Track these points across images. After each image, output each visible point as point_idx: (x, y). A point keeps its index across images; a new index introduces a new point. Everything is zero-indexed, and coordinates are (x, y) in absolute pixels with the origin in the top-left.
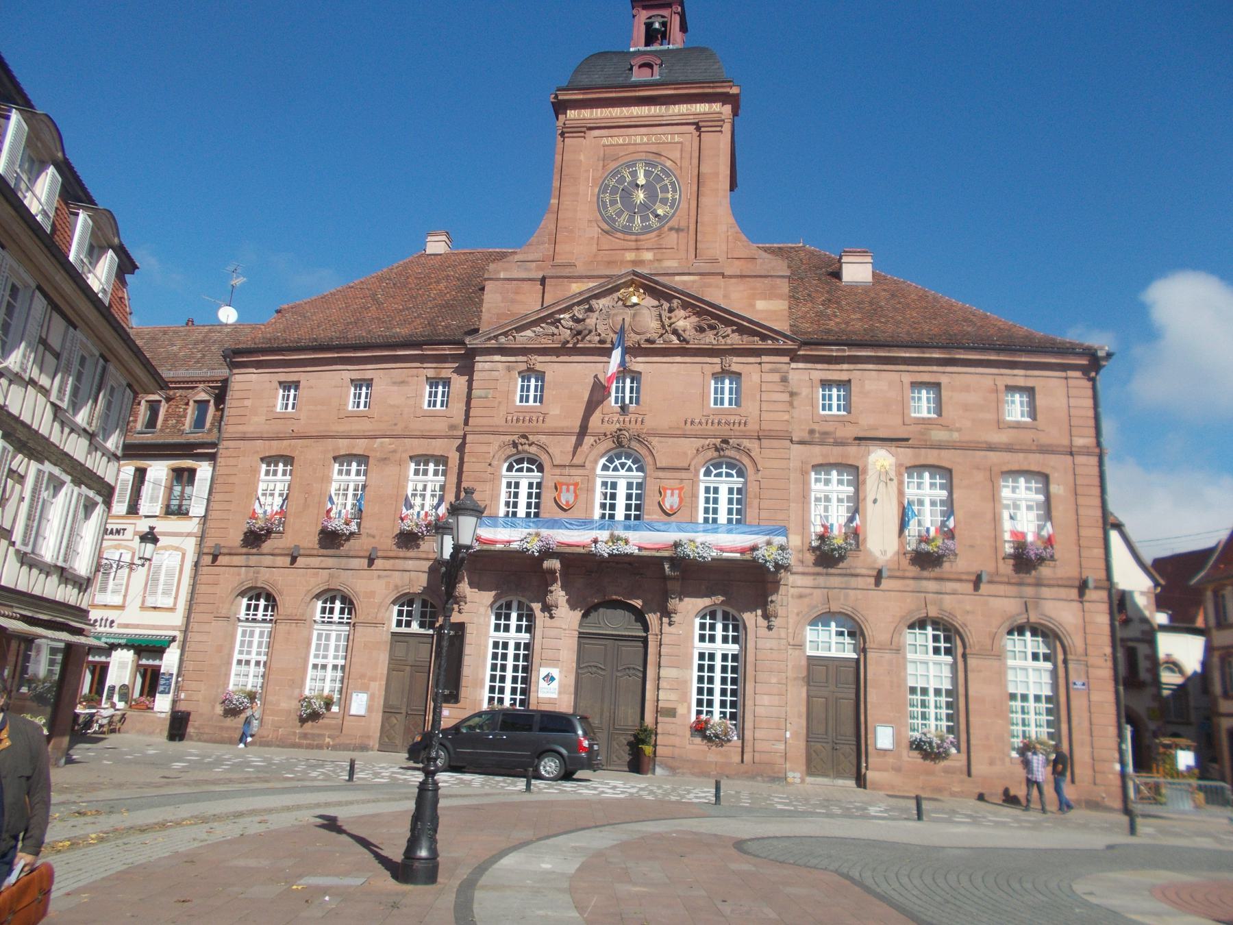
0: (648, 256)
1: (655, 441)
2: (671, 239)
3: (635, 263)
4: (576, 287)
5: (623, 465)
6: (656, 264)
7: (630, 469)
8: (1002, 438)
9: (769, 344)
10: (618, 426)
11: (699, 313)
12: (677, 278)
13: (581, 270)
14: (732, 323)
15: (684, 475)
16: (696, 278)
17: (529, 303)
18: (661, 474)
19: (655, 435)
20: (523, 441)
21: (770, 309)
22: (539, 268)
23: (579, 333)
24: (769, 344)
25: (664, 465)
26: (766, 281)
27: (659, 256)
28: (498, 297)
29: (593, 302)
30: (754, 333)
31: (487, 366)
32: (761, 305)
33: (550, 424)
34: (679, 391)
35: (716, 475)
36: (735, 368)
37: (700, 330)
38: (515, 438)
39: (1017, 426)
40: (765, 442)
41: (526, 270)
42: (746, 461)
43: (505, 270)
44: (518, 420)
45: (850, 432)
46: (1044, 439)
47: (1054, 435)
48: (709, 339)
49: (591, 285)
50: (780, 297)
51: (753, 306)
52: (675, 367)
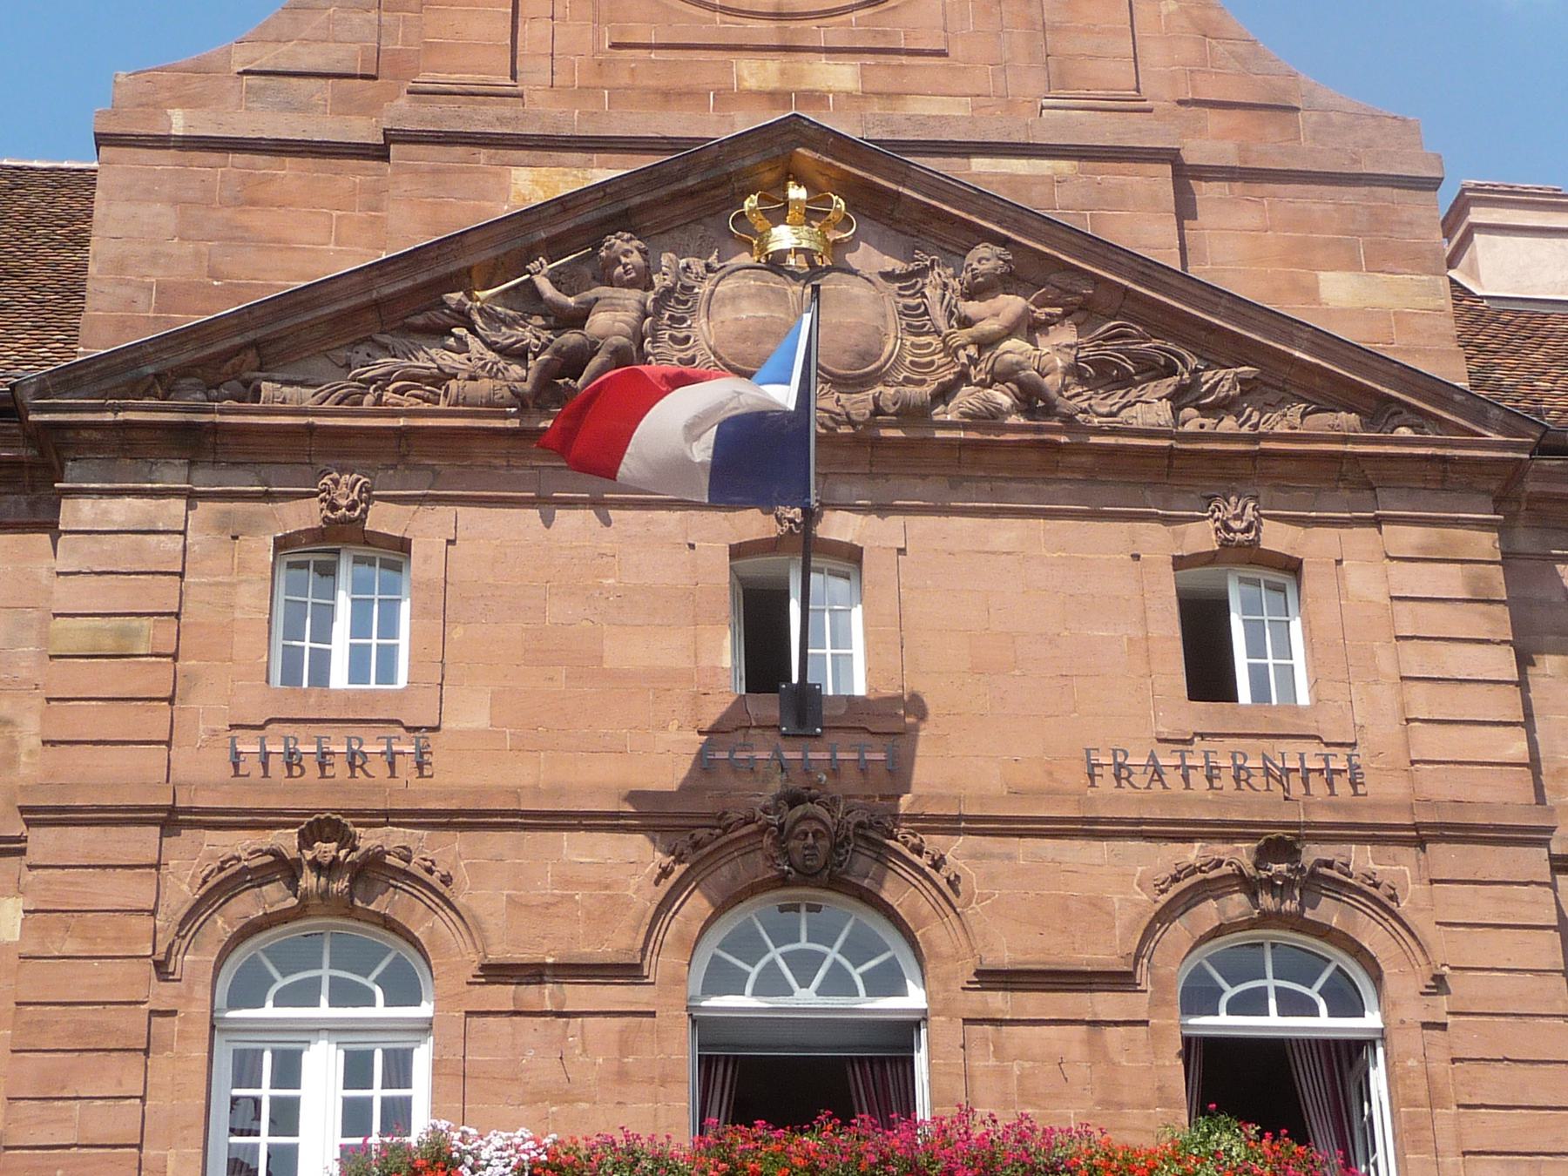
0: (839, 76)
1: (955, 849)
3: (774, 97)
4: (531, 184)
5: (805, 966)
6: (876, 108)
7: (838, 983)
10: (775, 786)
11: (1082, 312)
12: (980, 164)
13: (544, 111)
14: (1240, 350)
15: (1105, 1004)
16: (1065, 166)
17: (325, 236)
18: (998, 1002)
19: (952, 825)
20: (326, 850)
22: (344, 106)
23: (573, 362)
25: (1004, 956)
26: (1350, 194)
27: (883, 80)
28: (161, 215)
29: (625, 248)
30: (1327, 392)
31: (122, 511)
33: (457, 776)
35: (1235, 1008)
37: (1102, 374)
38: (286, 841)
40: (1447, 857)
41: (290, 107)
42: (1373, 935)
43: (186, 102)
44: (292, 760)
48: (1150, 409)
49: (601, 171)
50: (1415, 260)
51: (1311, 293)
52: (1007, 533)
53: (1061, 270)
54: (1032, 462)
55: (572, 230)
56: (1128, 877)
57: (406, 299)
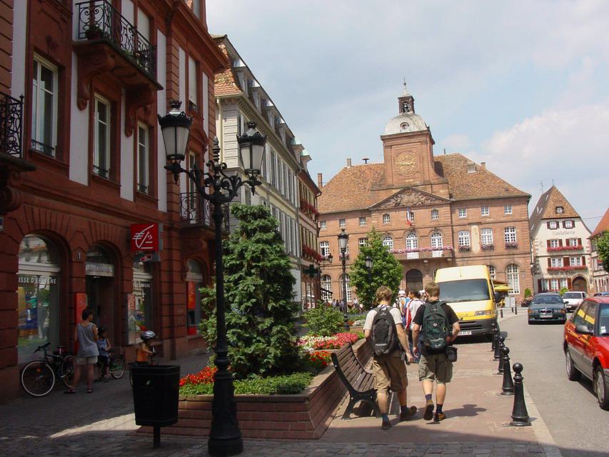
0: (412, 180)
2: (417, 175)
4: (395, 191)
8: (503, 219)
9: (444, 202)
13: (396, 185)
21: (442, 192)
24: (444, 202)
29: (399, 195)
32: (441, 191)
33: (392, 228)
34: (423, 217)
36: (437, 209)
39: (508, 215)
45: (466, 222)
46: (514, 219)
47: (517, 217)
48: (429, 202)
49: (398, 190)
53: (424, 194)
54: (423, 206)
55: (396, 195)
56: (428, 230)
57: (388, 200)
